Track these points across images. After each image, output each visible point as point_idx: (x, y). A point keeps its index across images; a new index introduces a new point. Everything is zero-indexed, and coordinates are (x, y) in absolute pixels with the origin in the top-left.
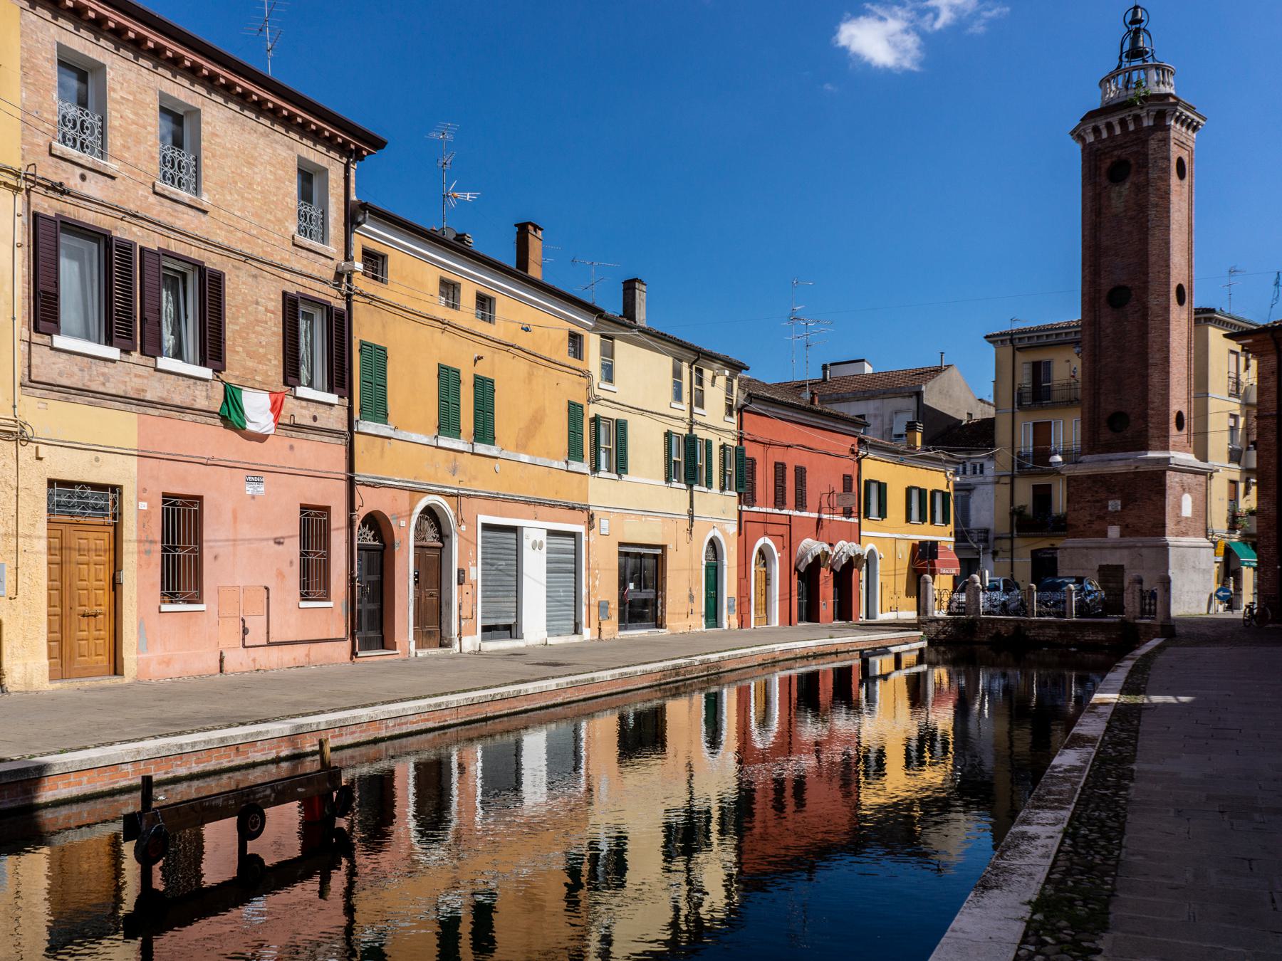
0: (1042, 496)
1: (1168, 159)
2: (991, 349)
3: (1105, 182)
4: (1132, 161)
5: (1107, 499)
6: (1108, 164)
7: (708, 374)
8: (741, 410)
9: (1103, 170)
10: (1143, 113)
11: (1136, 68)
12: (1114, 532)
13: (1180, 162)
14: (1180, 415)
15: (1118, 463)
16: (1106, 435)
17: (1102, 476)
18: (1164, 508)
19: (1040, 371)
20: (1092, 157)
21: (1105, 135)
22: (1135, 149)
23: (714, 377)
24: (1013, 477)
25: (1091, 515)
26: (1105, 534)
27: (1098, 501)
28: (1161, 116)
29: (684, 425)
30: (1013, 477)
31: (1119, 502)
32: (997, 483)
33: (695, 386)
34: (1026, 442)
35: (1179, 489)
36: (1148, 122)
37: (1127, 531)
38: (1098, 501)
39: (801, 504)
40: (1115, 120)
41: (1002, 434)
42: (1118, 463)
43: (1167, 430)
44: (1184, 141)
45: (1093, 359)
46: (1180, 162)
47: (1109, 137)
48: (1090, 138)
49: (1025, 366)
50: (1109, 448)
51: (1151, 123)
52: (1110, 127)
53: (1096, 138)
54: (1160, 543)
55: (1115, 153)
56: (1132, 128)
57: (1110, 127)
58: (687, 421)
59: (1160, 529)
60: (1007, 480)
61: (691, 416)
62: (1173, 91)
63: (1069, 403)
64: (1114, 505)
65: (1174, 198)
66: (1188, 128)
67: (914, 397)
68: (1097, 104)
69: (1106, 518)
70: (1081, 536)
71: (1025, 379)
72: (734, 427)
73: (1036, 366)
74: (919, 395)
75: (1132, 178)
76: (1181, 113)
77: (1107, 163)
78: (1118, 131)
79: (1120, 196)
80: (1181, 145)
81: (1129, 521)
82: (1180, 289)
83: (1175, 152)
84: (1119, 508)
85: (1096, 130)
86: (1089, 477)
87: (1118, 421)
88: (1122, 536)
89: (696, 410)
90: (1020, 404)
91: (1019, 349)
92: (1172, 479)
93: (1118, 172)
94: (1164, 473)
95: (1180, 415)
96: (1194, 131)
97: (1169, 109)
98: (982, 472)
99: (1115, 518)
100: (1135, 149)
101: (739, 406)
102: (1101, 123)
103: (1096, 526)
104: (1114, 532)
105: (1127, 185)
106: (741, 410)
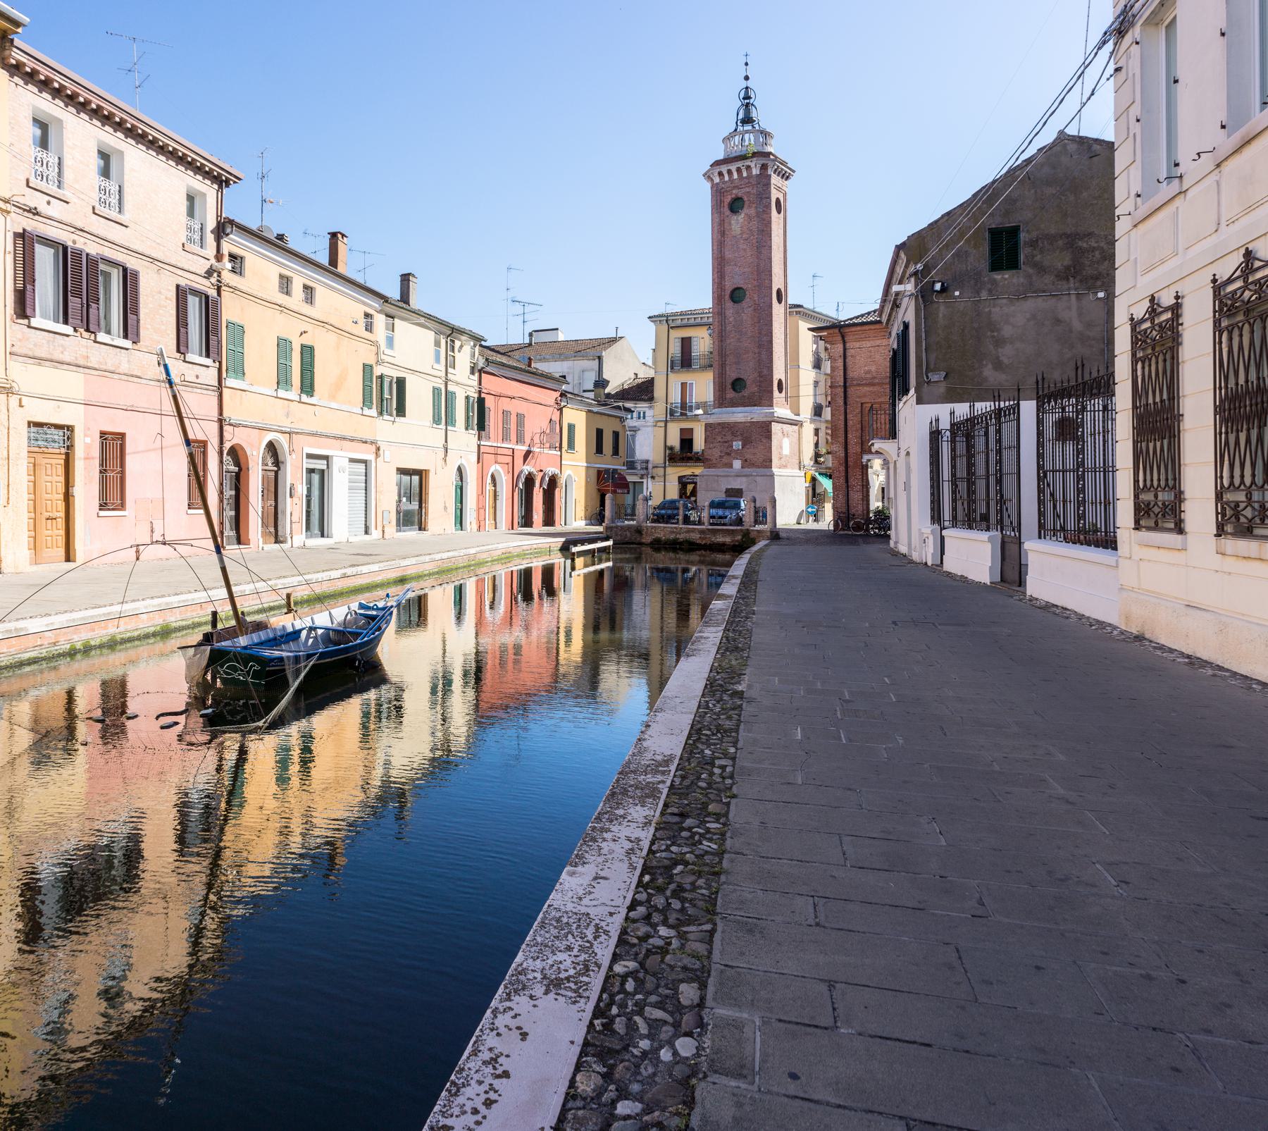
1: (769, 198)
2: (652, 326)
3: (728, 212)
4: (746, 199)
5: (732, 441)
6: (729, 199)
7: (457, 344)
8: (480, 371)
9: (726, 204)
10: (753, 165)
11: (747, 132)
12: (737, 464)
13: (778, 201)
14: (780, 382)
15: (739, 415)
16: (730, 394)
17: (728, 424)
18: (771, 448)
19: (686, 343)
21: (727, 178)
22: (747, 190)
23: (461, 347)
24: (666, 422)
25: (721, 452)
26: (731, 466)
27: (726, 442)
29: (440, 381)
30: (666, 422)
31: (740, 443)
32: (655, 426)
33: (449, 353)
34: (676, 397)
35: (780, 434)
36: (755, 171)
38: (726, 442)
40: (733, 167)
41: (659, 391)
42: (739, 415)
43: (771, 392)
44: (780, 186)
45: (720, 337)
46: (778, 201)
47: (729, 180)
48: (717, 180)
49: (677, 340)
51: (758, 173)
52: (730, 172)
53: (721, 180)
54: (768, 474)
55: (734, 192)
56: (745, 174)
57: (730, 172)
58: (444, 379)
59: (768, 463)
60: (663, 424)
61: (446, 375)
62: (773, 151)
63: (705, 368)
64: (737, 445)
65: (774, 226)
66: (782, 178)
67: (597, 360)
68: (721, 157)
70: (714, 467)
71: (676, 349)
72: (476, 383)
74: (600, 358)
75: (745, 210)
76: (778, 166)
77: (728, 199)
78: (735, 176)
79: (737, 223)
80: (779, 189)
81: (748, 456)
82: (779, 292)
83: (775, 194)
84: (740, 447)
85: (720, 174)
86: (719, 424)
87: (738, 384)
88: (742, 467)
89: (450, 370)
90: (672, 368)
91: (672, 327)
92: (776, 428)
93: (736, 205)
94: (770, 422)
95: (780, 382)
96: (786, 180)
97: (770, 164)
98: (644, 417)
99: (738, 454)
100: (747, 190)
101: (479, 368)
102: (724, 169)
103: (725, 460)
104: (737, 464)
105: (743, 215)
106: (480, 371)
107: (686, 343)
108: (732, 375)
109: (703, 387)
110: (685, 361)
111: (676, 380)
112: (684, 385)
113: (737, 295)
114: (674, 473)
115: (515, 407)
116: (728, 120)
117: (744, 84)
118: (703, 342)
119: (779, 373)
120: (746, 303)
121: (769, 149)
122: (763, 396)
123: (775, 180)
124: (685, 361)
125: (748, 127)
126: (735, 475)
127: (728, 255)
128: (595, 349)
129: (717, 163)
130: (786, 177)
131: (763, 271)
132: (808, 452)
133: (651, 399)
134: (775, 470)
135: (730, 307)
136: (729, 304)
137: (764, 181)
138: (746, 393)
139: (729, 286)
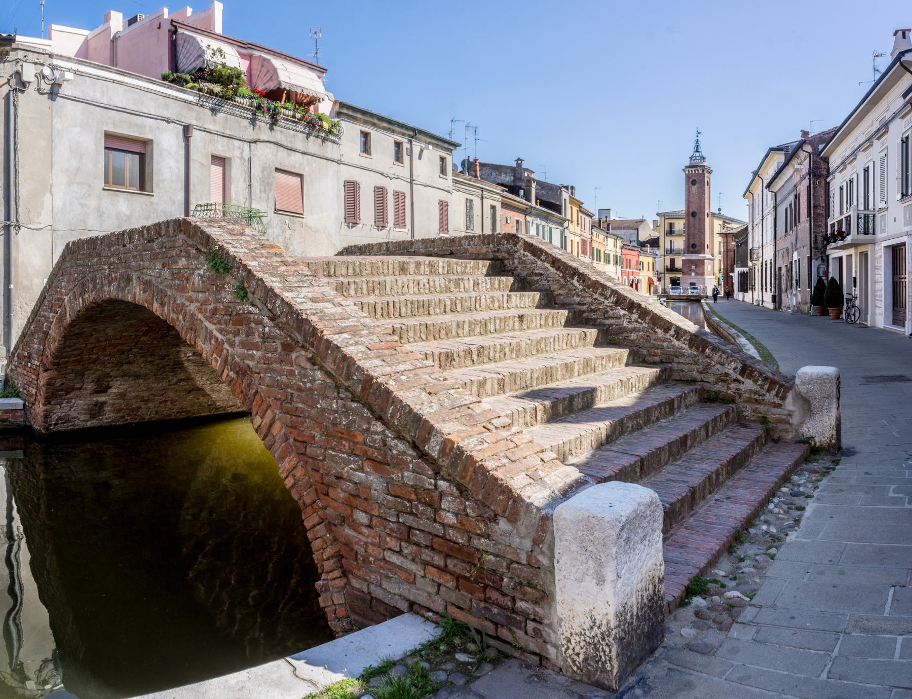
0: (672, 261)
12: (693, 274)
15: (694, 257)
16: (691, 249)
19: (671, 225)
20: (688, 177)
28: (703, 171)
34: (668, 247)
36: (700, 172)
37: (696, 274)
39: (630, 268)
40: (693, 169)
42: (694, 257)
45: (688, 226)
50: (692, 253)
59: (703, 274)
63: (680, 235)
64: (693, 267)
68: (688, 164)
69: (691, 270)
71: (667, 227)
73: (671, 224)
79: (694, 188)
83: (706, 180)
87: (694, 246)
93: (694, 183)
99: (693, 271)
102: (690, 169)
104: (693, 274)
107: (671, 225)
108: (692, 242)
109: (679, 243)
110: (671, 232)
111: (668, 239)
112: (671, 241)
113: (694, 214)
114: (668, 276)
115: (629, 257)
116: (691, 152)
117: (696, 138)
118: (679, 225)
119: (707, 242)
120: (697, 217)
121: (705, 164)
122: (701, 250)
123: (707, 175)
124: (671, 232)
125: (697, 154)
126: (693, 276)
127: (691, 200)
128: (636, 225)
129: (687, 167)
130: (710, 173)
131: (702, 207)
132: (717, 270)
133: (658, 247)
134: (706, 276)
135: (691, 219)
136: (691, 217)
137: (703, 174)
138: (696, 249)
139: (691, 210)
